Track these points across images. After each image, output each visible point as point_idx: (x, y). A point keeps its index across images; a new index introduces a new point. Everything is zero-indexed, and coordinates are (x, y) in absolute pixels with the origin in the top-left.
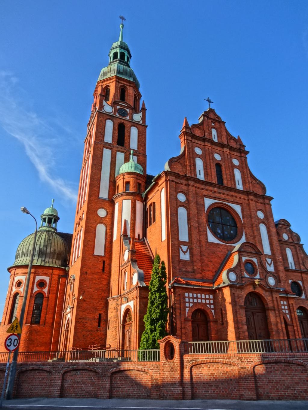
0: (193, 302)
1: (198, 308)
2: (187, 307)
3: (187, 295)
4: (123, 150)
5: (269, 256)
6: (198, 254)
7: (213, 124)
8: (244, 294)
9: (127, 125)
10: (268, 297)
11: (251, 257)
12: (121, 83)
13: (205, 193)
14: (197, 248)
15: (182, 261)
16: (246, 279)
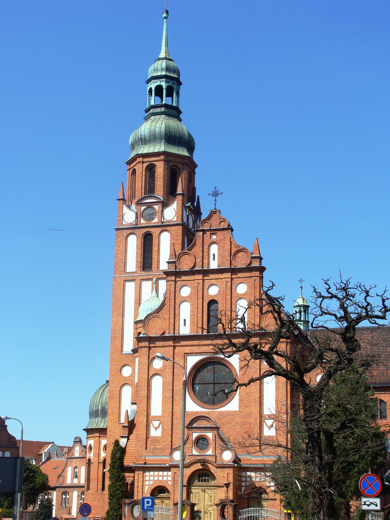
0: (154, 480)
1: (158, 485)
2: (147, 485)
3: (147, 474)
4: (149, 277)
5: (270, 417)
6: (169, 428)
7: (214, 237)
8: (188, 472)
9: (155, 232)
10: (218, 473)
11: (204, 431)
12: (147, 162)
13: (187, 350)
14: (168, 421)
15: (151, 438)
16: (192, 457)
